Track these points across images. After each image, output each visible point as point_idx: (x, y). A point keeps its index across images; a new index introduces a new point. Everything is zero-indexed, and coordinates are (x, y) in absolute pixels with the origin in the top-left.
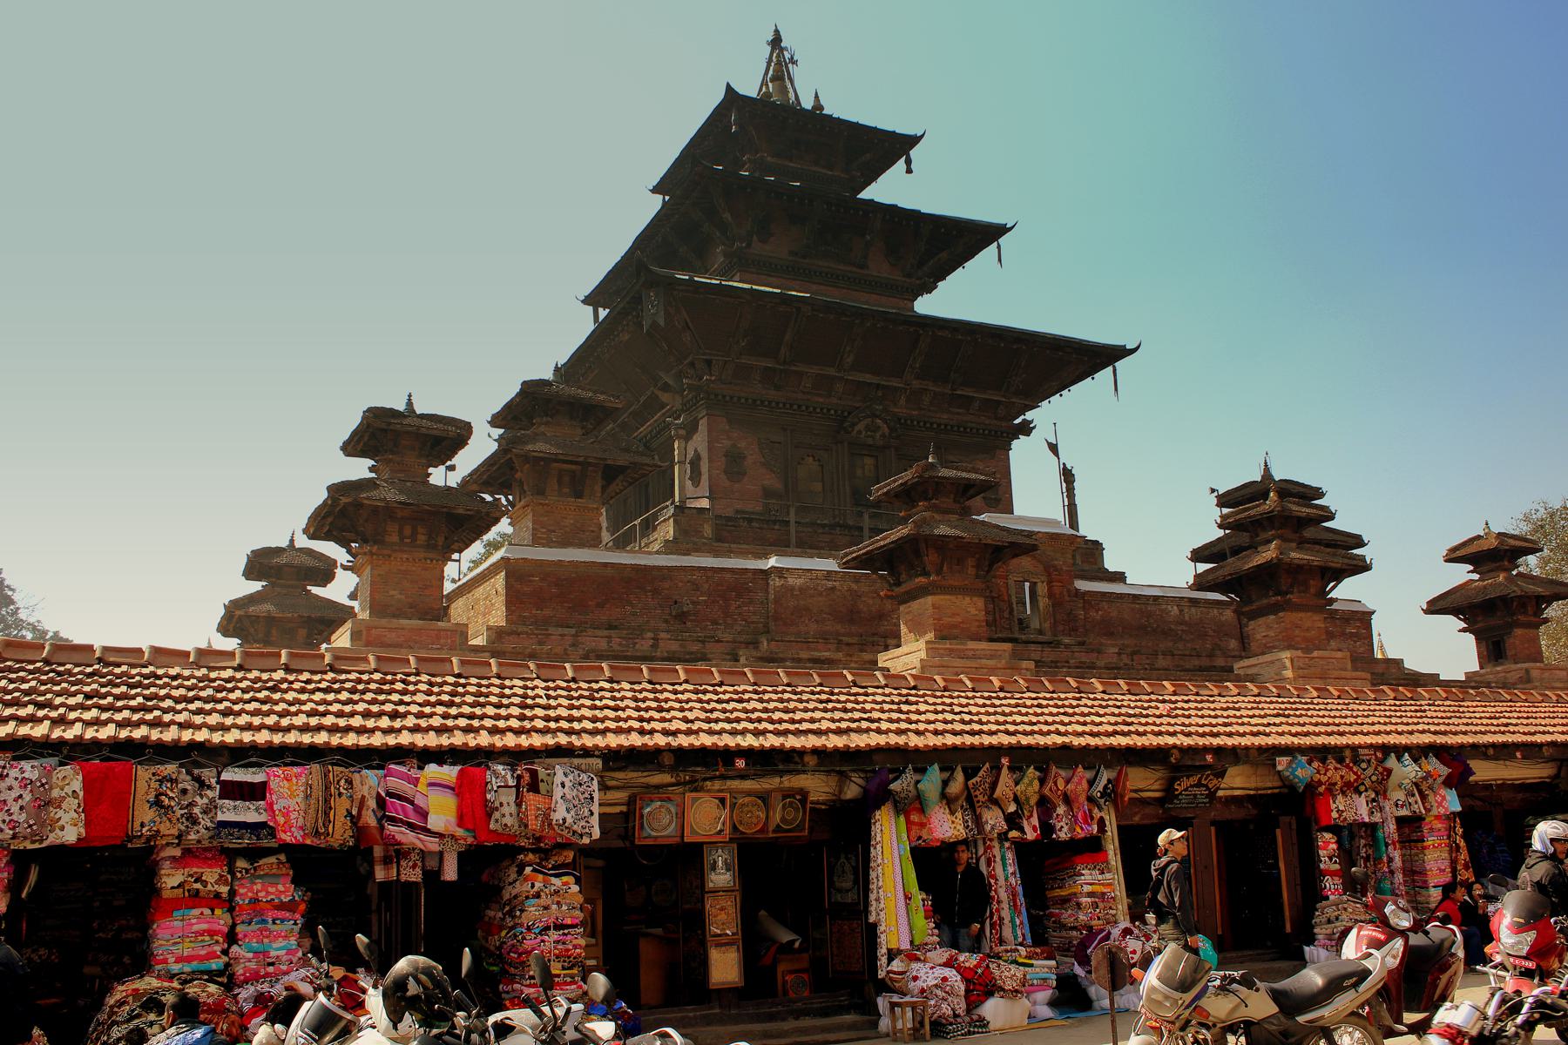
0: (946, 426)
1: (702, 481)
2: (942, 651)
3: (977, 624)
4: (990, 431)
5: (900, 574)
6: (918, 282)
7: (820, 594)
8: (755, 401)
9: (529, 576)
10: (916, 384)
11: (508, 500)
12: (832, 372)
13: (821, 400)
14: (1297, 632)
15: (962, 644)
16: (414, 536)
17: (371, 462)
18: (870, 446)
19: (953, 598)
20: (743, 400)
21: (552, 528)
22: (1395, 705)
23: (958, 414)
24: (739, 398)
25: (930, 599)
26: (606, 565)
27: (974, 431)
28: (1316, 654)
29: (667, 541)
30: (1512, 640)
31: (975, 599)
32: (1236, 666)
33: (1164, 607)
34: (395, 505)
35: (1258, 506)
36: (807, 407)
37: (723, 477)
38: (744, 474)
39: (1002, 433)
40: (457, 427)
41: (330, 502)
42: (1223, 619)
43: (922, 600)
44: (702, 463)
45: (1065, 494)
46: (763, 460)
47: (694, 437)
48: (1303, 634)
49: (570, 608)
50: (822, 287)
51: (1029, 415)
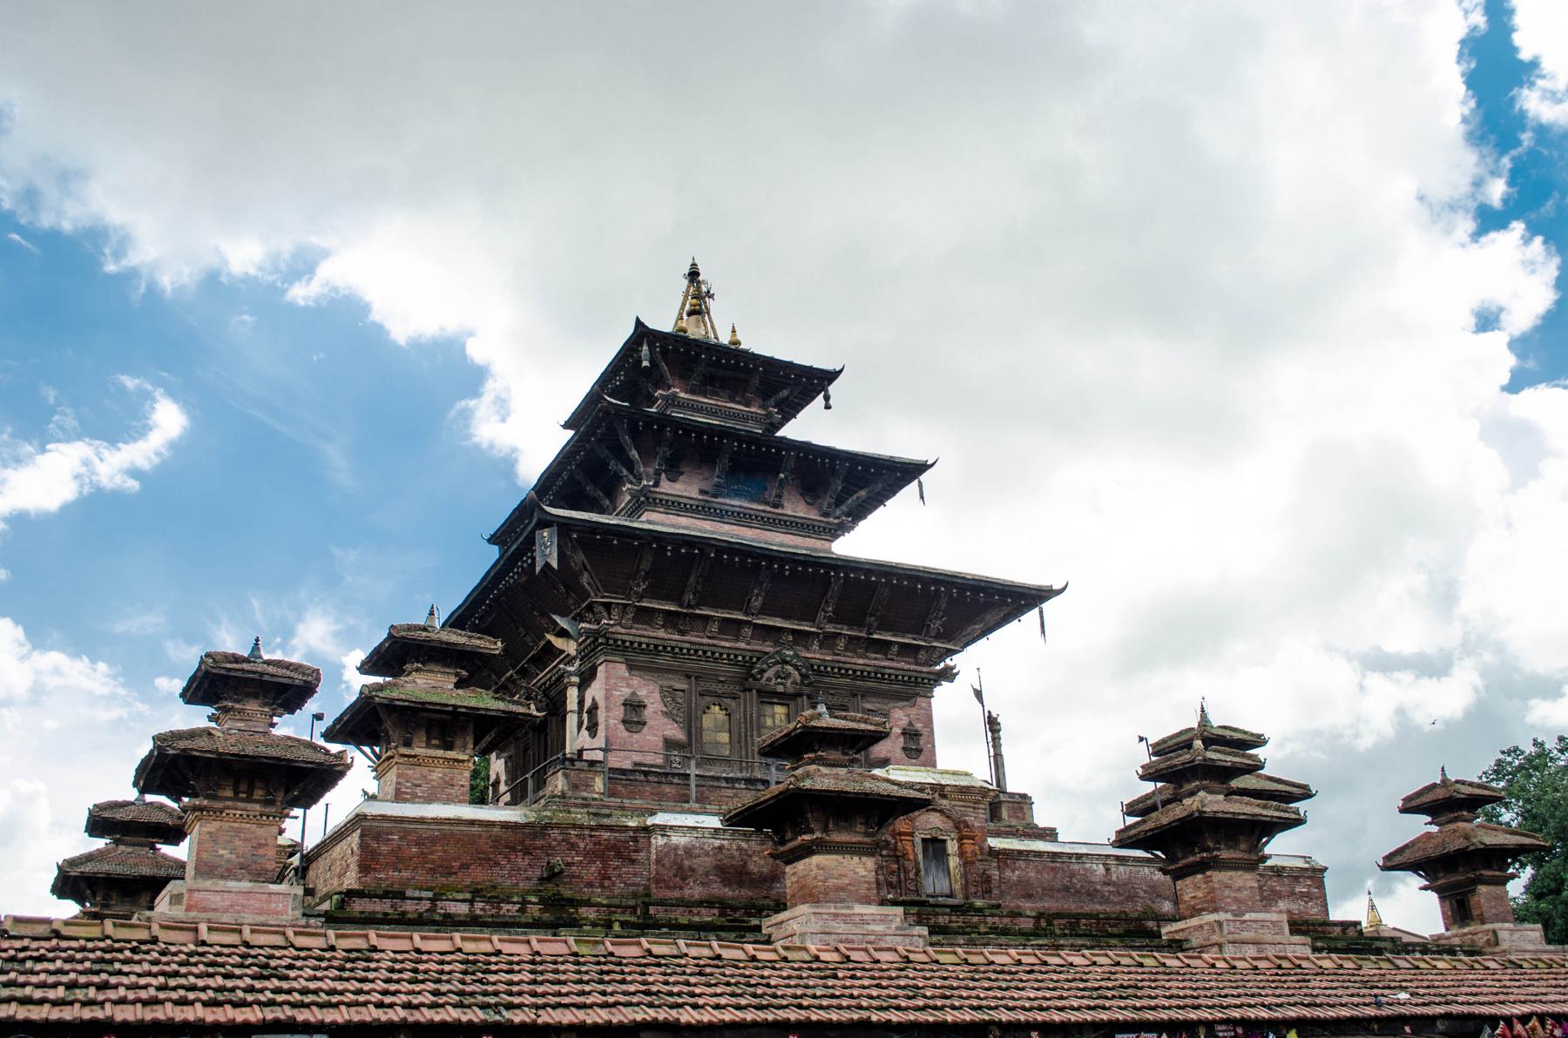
1: (599, 731)
2: (826, 917)
4: (910, 677)
5: (785, 832)
6: (836, 521)
7: (707, 854)
9: (387, 834)
10: (830, 628)
11: (373, 752)
13: (727, 644)
14: (1227, 893)
15: (848, 907)
16: (250, 792)
17: (210, 710)
19: (840, 858)
20: (644, 646)
21: (418, 782)
22: (1277, 974)
24: (640, 644)
27: (893, 677)
28: (1247, 916)
30: (1477, 899)
31: (864, 859)
32: (1164, 931)
33: (1088, 866)
36: (713, 653)
37: (622, 727)
38: (644, 724)
39: (923, 679)
40: (304, 674)
41: (156, 753)
43: (807, 860)
44: (599, 712)
45: (991, 744)
46: (664, 709)
47: (593, 685)
48: (1233, 895)
49: (431, 869)
50: (735, 527)
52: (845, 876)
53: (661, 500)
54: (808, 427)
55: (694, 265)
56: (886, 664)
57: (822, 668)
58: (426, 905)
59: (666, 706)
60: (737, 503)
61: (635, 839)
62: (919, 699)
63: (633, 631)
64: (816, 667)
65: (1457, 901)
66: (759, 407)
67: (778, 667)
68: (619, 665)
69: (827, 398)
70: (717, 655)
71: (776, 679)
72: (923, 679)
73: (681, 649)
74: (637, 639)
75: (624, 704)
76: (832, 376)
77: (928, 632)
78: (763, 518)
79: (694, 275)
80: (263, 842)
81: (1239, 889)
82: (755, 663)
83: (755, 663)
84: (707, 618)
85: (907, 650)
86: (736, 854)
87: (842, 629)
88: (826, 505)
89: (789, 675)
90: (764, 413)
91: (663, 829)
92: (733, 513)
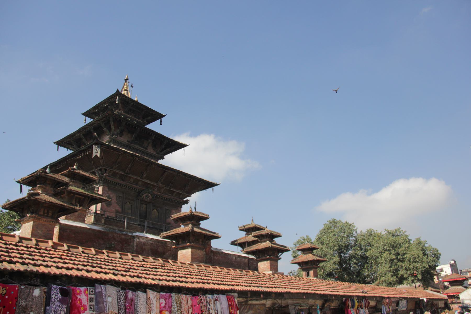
6: (160, 156)
8: (117, 183)
12: (139, 178)
18: (146, 201)
20: (114, 183)
23: (169, 195)
24: (113, 182)
29: (92, 223)
31: (201, 251)
33: (232, 257)
34: (48, 202)
35: (262, 232)
36: (131, 188)
38: (111, 205)
39: (181, 202)
42: (245, 261)
51: (188, 198)
53: (117, 142)
59: (117, 200)
60: (136, 146)
61: (130, 239)
65: (307, 272)
66: (142, 120)
67: (147, 194)
69: (161, 122)
70: (132, 188)
72: (181, 202)
76: (164, 116)
77: (184, 190)
78: (142, 151)
80: (50, 229)
83: (141, 192)
84: (130, 178)
86: (155, 246)
88: (158, 151)
90: (143, 122)
91: (139, 237)
92: (135, 149)
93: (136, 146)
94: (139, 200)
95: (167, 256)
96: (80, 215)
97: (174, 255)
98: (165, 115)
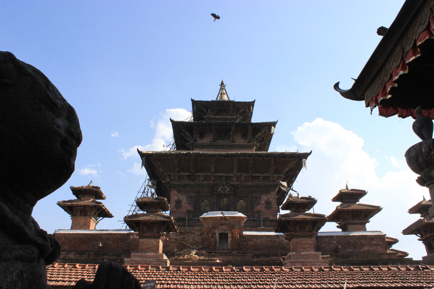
0: (250, 186)
2: (137, 256)
3: (156, 247)
4: (267, 186)
9: (61, 238)
10: (238, 174)
12: (209, 174)
13: (206, 182)
19: (148, 240)
20: (181, 185)
21: (77, 225)
24: (180, 185)
25: (288, 241)
26: (82, 234)
28: (303, 253)
31: (156, 239)
33: (281, 239)
37: (174, 208)
46: (188, 202)
48: (301, 246)
52: (149, 245)
54: (255, 119)
55: (222, 81)
56: (259, 183)
57: (237, 186)
58: (65, 255)
59: (188, 201)
62: (271, 192)
63: (179, 182)
64: (235, 186)
67: (222, 187)
68: (174, 191)
71: (222, 190)
72: (272, 186)
73: (192, 185)
74: (179, 184)
75: (175, 202)
79: (222, 83)
81: (304, 244)
82: (215, 187)
83: (215, 187)
84: (199, 176)
85: (265, 178)
87: (242, 174)
88: (248, 139)
89: (225, 189)
92: (219, 146)
93: (220, 142)
94: (215, 195)
95: (171, 249)
96: (84, 224)
97: (180, 247)
98: (254, 102)
